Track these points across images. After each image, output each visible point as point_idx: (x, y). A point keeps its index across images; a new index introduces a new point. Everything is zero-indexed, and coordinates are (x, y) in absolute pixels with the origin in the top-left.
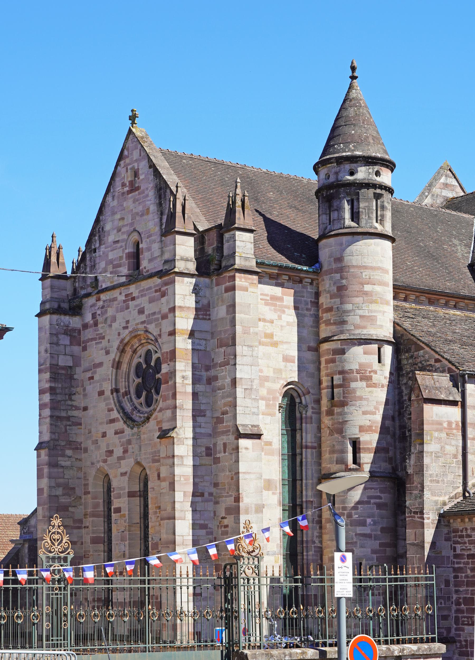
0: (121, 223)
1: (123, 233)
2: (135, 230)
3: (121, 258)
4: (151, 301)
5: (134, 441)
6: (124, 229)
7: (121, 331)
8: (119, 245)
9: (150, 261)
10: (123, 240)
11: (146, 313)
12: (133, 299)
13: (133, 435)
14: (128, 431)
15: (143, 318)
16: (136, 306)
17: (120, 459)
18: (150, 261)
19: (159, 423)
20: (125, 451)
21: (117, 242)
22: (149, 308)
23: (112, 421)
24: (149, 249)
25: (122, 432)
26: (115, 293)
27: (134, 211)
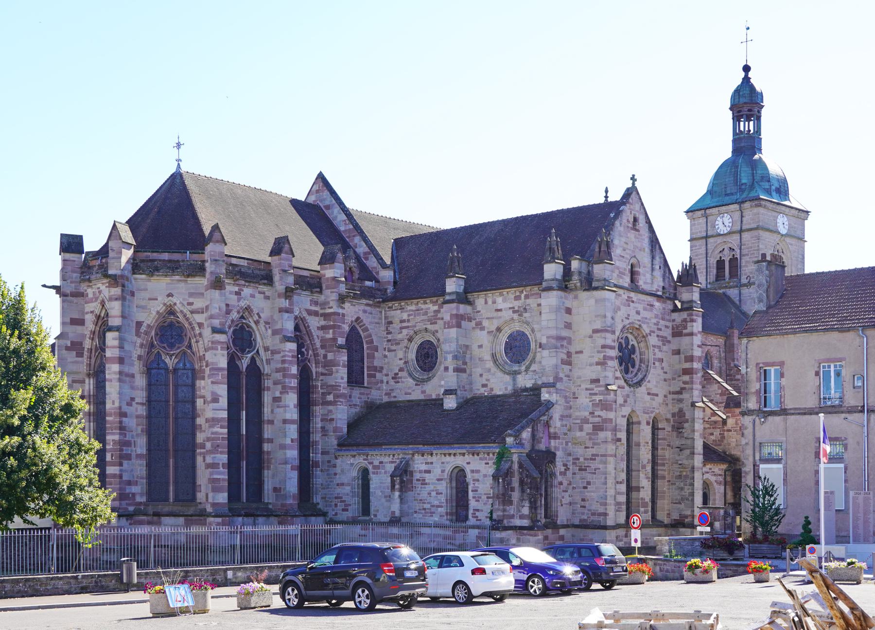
0: (625, 246)
1: (627, 253)
2: (635, 257)
3: (625, 269)
4: (645, 309)
5: (631, 396)
6: (627, 251)
7: (624, 319)
8: (624, 260)
9: (645, 283)
10: (627, 258)
11: (641, 315)
12: (633, 302)
13: (631, 392)
14: (627, 388)
15: (639, 317)
16: (635, 308)
17: (621, 405)
18: (645, 283)
19: (647, 389)
20: (625, 401)
21: (623, 257)
22: (645, 314)
23: (617, 378)
24: (644, 276)
25: (623, 388)
26: (621, 291)
27: (635, 244)
